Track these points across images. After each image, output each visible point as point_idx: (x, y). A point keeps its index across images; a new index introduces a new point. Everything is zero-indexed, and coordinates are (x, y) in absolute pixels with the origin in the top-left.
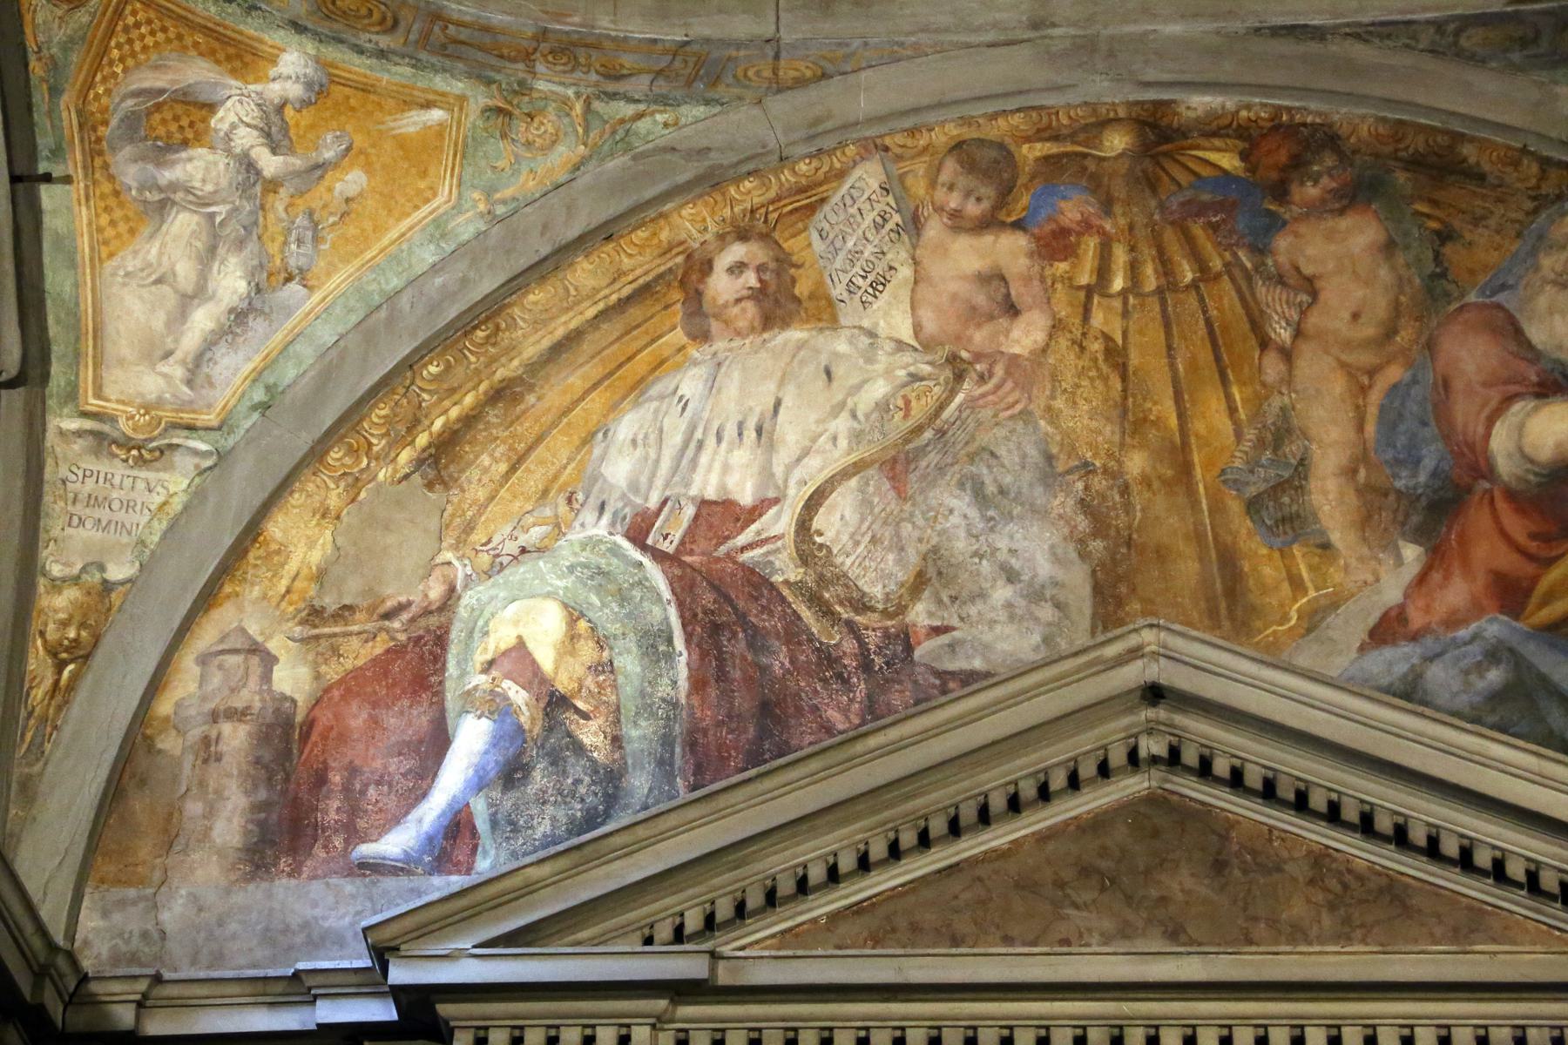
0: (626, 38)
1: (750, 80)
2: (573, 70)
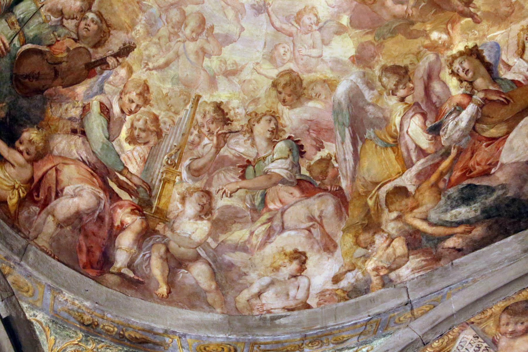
0: (343, 327)
1: (402, 321)
2: (321, 346)
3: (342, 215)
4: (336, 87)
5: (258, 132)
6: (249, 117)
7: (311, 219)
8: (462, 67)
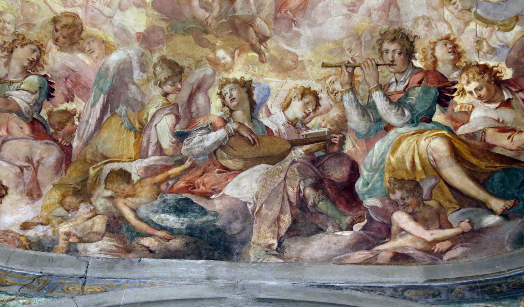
0: (11, 272)
1: (69, 291)
3: (60, 171)
4: (111, 52)
5: (18, 55)
6: (16, 38)
7: (29, 160)
8: (230, 93)
